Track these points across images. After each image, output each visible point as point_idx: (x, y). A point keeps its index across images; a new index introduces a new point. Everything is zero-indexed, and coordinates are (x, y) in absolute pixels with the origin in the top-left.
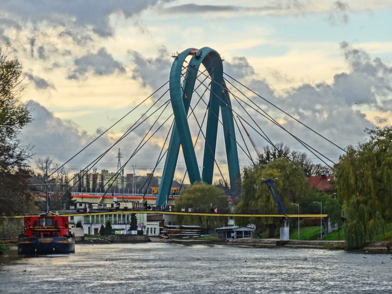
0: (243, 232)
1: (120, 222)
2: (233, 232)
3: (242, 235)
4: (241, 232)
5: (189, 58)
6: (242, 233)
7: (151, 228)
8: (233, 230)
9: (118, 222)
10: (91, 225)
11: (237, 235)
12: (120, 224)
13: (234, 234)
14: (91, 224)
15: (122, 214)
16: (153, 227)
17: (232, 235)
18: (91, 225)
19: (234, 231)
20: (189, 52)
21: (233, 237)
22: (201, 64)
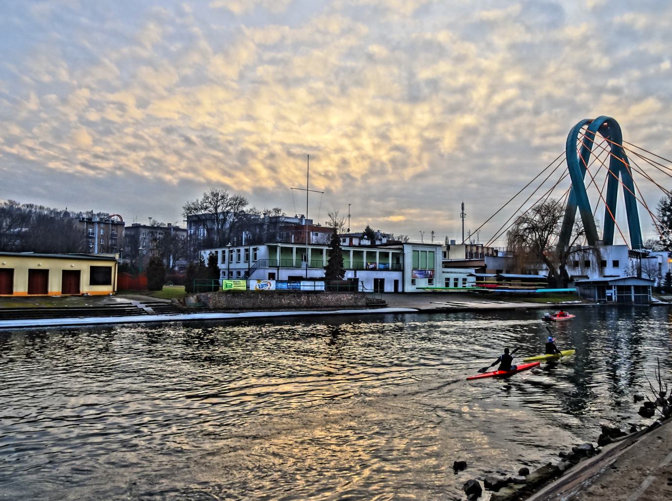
0: (632, 288)
1: (371, 266)
2: (610, 288)
3: (631, 293)
4: (628, 288)
5: (586, 127)
6: (630, 290)
7: (456, 279)
8: (610, 284)
9: (367, 264)
10: (278, 270)
11: (618, 293)
12: (374, 269)
13: (612, 291)
14: (278, 268)
15: (391, 252)
16: (455, 276)
17: (608, 293)
18: (278, 270)
19: (611, 286)
20: (588, 122)
21: (610, 298)
22: (598, 133)
